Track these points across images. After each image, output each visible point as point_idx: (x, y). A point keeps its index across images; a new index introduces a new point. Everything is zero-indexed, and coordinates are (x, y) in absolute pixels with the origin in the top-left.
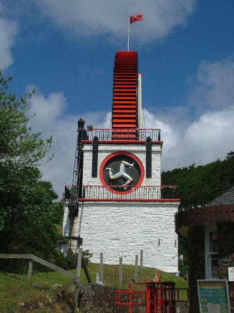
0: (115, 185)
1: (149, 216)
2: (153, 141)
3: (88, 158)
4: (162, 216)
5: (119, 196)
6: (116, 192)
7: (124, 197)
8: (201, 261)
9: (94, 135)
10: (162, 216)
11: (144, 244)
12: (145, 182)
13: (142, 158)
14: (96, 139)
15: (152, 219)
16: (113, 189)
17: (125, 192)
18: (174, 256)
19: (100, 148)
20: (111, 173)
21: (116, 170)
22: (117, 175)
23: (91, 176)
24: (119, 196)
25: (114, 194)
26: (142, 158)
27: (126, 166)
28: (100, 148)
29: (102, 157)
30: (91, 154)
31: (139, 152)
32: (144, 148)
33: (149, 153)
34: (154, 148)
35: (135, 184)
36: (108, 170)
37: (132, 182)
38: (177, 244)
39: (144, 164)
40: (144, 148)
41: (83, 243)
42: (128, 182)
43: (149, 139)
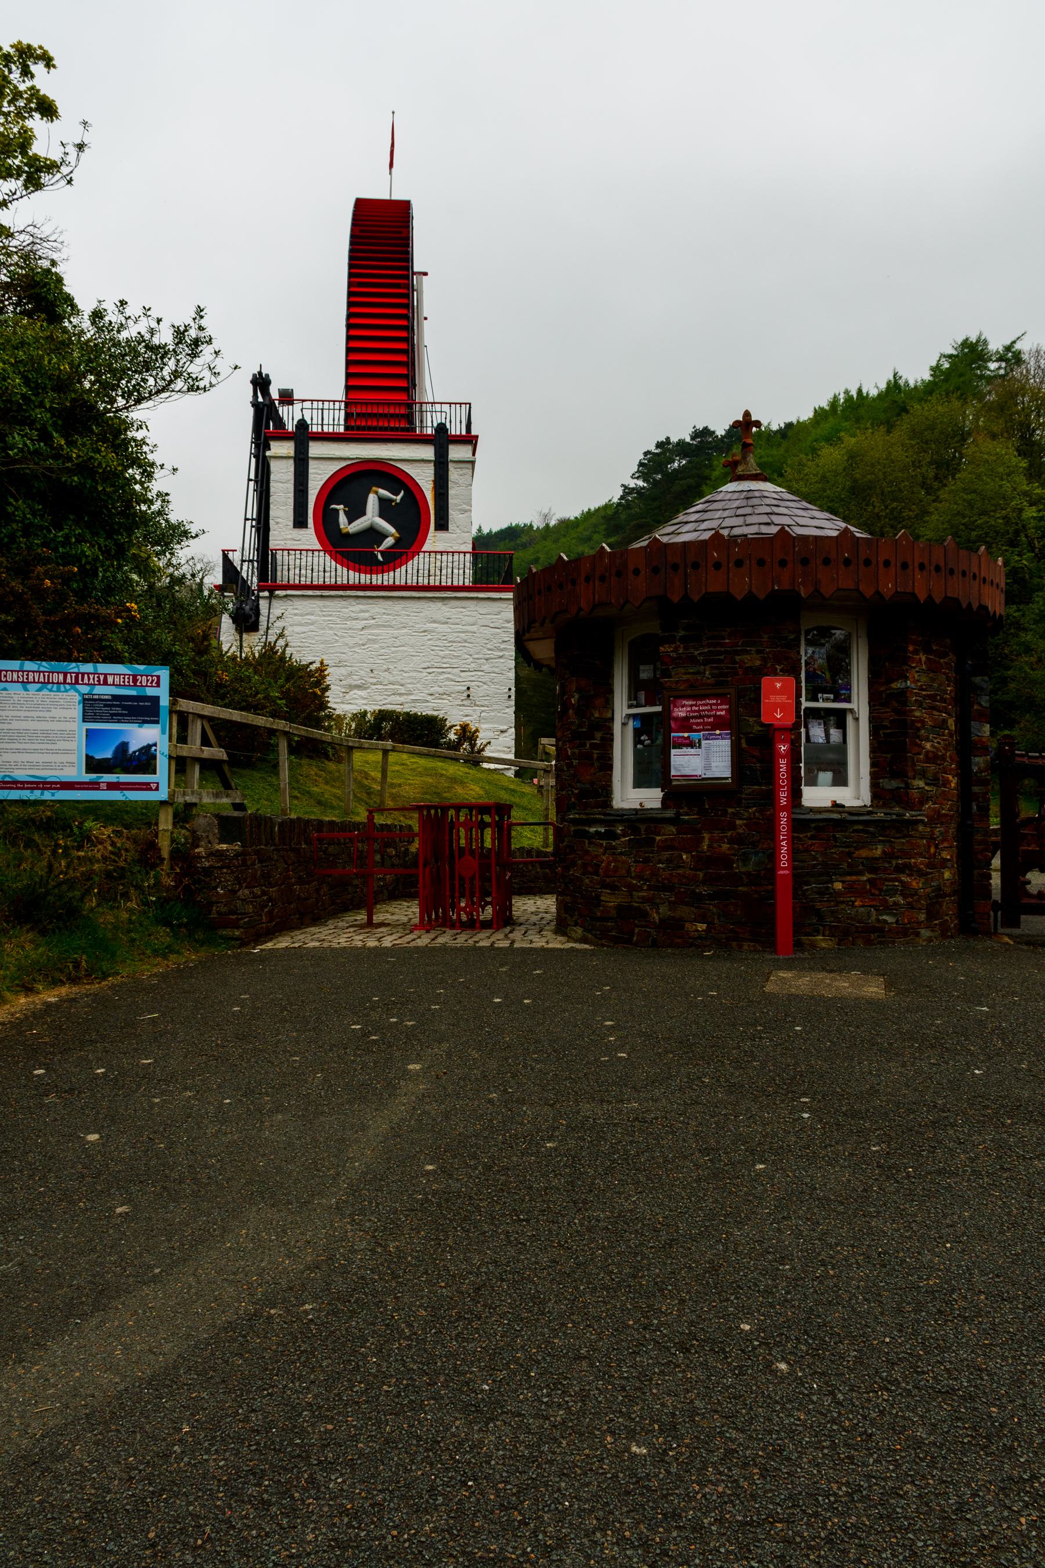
0: (353, 550)
2: (453, 433)
3: (282, 475)
4: (474, 628)
5: (365, 579)
6: (357, 566)
7: (377, 579)
8: (598, 735)
9: (298, 417)
10: (474, 628)
11: (429, 698)
12: (434, 541)
13: (424, 478)
14: (302, 425)
15: (451, 637)
16: (342, 553)
17: (380, 568)
18: (505, 727)
19: (315, 449)
20: (343, 519)
21: (356, 511)
23: (291, 524)
24: (365, 579)
25: (351, 572)
26: (424, 478)
27: (383, 502)
28: (315, 449)
29: (319, 476)
30: (289, 467)
31: (414, 460)
32: (428, 452)
33: (441, 466)
34: (456, 452)
35: (410, 543)
36: (337, 511)
37: (398, 540)
38: (513, 697)
40: (428, 452)
43: (441, 428)
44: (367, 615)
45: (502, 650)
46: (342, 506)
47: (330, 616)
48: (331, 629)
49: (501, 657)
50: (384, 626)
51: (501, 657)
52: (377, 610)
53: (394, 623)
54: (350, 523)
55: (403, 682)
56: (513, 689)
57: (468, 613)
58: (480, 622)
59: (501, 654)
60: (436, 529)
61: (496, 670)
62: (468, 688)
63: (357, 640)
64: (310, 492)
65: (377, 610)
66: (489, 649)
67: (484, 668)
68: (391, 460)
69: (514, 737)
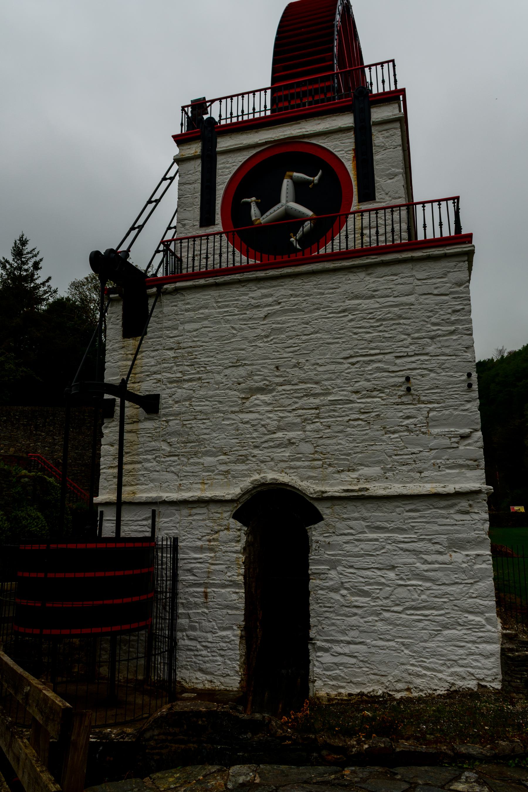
1: (370, 304)
2: (375, 92)
4: (411, 299)
10: (411, 299)
11: (354, 397)
13: (343, 149)
18: (468, 431)
19: (224, 143)
20: (254, 211)
21: (270, 199)
23: (198, 223)
27: (298, 185)
36: (249, 204)
38: (475, 387)
39: (350, 166)
40: (347, 120)
41: (162, 412)
42: (307, 225)
44: (270, 299)
45: (453, 323)
47: (227, 306)
48: (227, 322)
49: (452, 333)
50: (292, 311)
51: (452, 333)
52: (283, 292)
53: (304, 305)
54: (262, 213)
55: (318, 378)
56: (474, 375)
57: (400, 281)
59: (453, 328)
61: (447, 351)
62: (408, 379)
63: (258, 331)
64: (218, 187)
65: (283, 292)
66: (434, 324)
67: (430, 349)
68: (304, 136)
69: (481, 443)
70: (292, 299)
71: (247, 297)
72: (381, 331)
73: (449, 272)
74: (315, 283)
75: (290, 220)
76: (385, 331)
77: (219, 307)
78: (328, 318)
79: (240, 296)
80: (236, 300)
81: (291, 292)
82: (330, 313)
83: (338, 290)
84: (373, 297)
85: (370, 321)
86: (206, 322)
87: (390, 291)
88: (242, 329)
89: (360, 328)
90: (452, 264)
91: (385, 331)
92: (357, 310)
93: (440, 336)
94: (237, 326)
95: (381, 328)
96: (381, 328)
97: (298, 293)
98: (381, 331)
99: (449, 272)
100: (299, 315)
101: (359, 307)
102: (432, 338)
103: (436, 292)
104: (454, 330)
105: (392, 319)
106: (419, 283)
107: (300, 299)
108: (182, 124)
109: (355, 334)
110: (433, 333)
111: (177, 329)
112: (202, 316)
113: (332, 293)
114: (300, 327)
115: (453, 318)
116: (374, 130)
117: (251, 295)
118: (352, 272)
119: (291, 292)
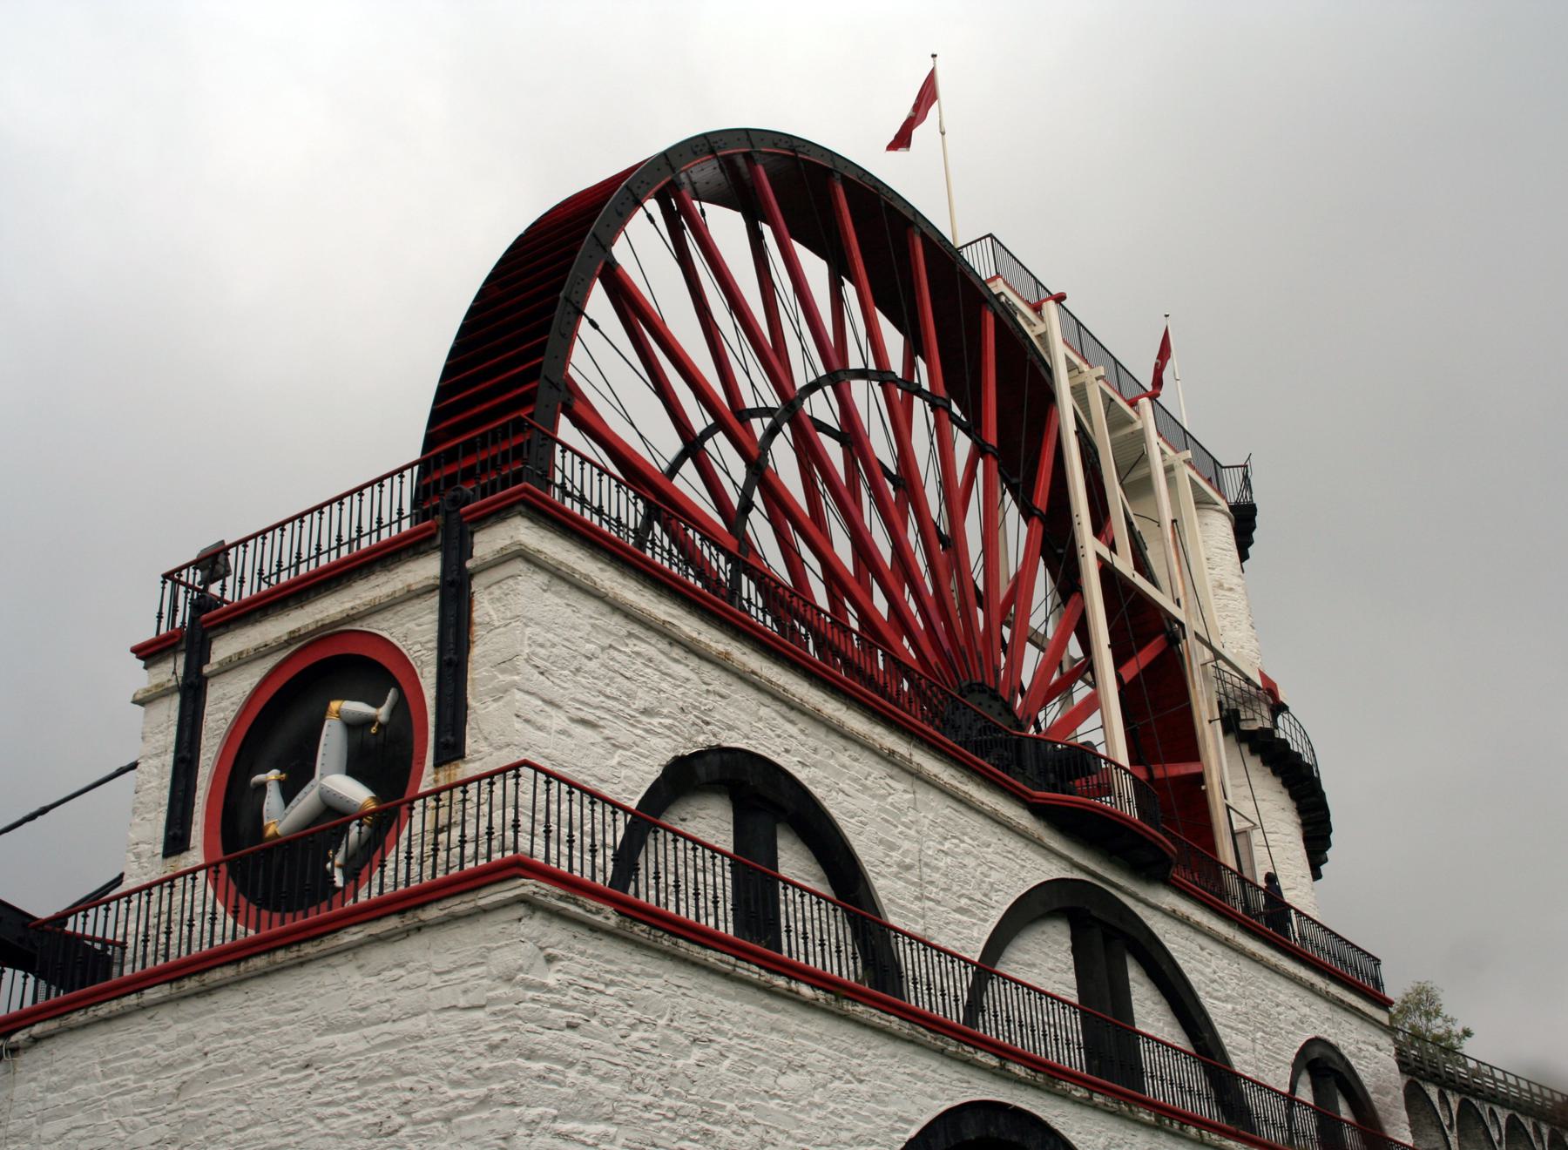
4: (420, 1023)
19: (223, 648)
22: (307, 800)
23: (160, 849)
26: (415, 635)
27: (355, 727)
36: (262, 787)
45: (486, 1079)
46: (273, 774)
48: (114, 1109)
49: (484, 1102)
50: (224, 1072)
51: (484, 1102)
57: (404, 981)
58: (437, 999)
59: (482, 1091)
60: (438, 764)
68: (350, 618)
70: (227, 1042)
71: (151, 1046)
72: (362, 1110)
73: (489, 950)
74: (266, 999)
75: (333, 815)
76: (369, 1109)
77: (105, 1075)
78: (278, 1085)
79: (142, 1044)
80: (136, 1055)
81: (226, 1026)
82: (283, 1072)
83: (302, 1014)
84: (358, 1024)
85: (348, 1085)
86: (79, 1115)
87: (387, 1005)
88: (135, 1127)
89: (328, 1104)
90: (493, 930)
91: (369, 1109)
92: (330, 1060)
93: (460, 1113)
94: (126, 1120)
95: (361, 1104)
96: (361, 1104)
97: (235, 1027)
98: (362, 1110)
99: (489, 950)
100: (233, 1081)
101: (333, 1051)
102: (447, 1120)
103: (462, 1002)
104: (487, 1096)
105: (383, 1078)
106: (436, 981)
107: (240, 1041)
108: (160, 616)
109: (321, 1120)
110: (450, 1107)
111: (28, 1137)
112: (74, 1100)
113: (292, 1022)
114: (230, 1111)
115: (486, 1065)
116: (477, 585)
117: (163, 1038)
118: (329, 965)
119: (226, 1026)
